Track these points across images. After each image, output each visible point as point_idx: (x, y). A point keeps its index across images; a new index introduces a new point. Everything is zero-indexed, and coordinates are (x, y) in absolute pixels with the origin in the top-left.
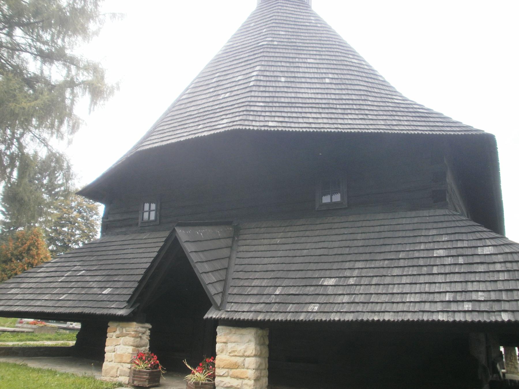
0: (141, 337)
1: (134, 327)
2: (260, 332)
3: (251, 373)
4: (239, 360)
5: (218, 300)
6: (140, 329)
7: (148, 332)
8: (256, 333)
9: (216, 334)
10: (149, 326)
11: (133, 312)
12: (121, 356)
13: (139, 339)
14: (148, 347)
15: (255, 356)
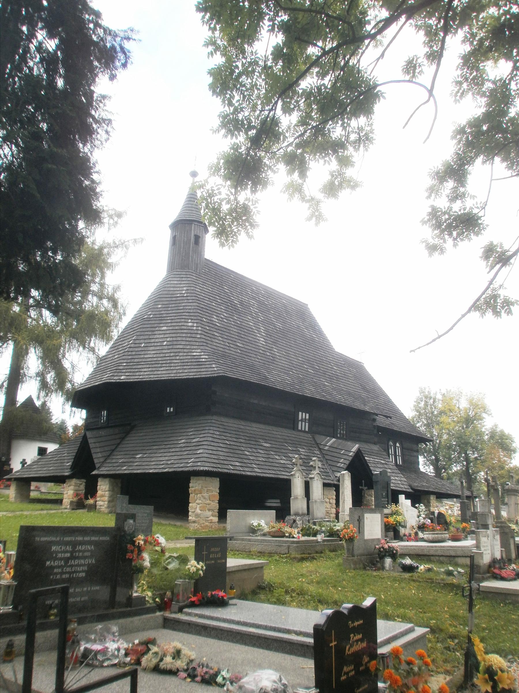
0: (79, 486)
1: (74, 481)
2: (112, 480)
3: (106, 498)
4: (104, 493)
5: (97, 466)
6: (78, 482)
7: (84, 484)
8: (110, 480)
9: (97, 482)
10: (85, 481)
11: (72, 474)
12: (69, 495)
13: (77, 487)
14: (84, 491)
15: (109, 491)
